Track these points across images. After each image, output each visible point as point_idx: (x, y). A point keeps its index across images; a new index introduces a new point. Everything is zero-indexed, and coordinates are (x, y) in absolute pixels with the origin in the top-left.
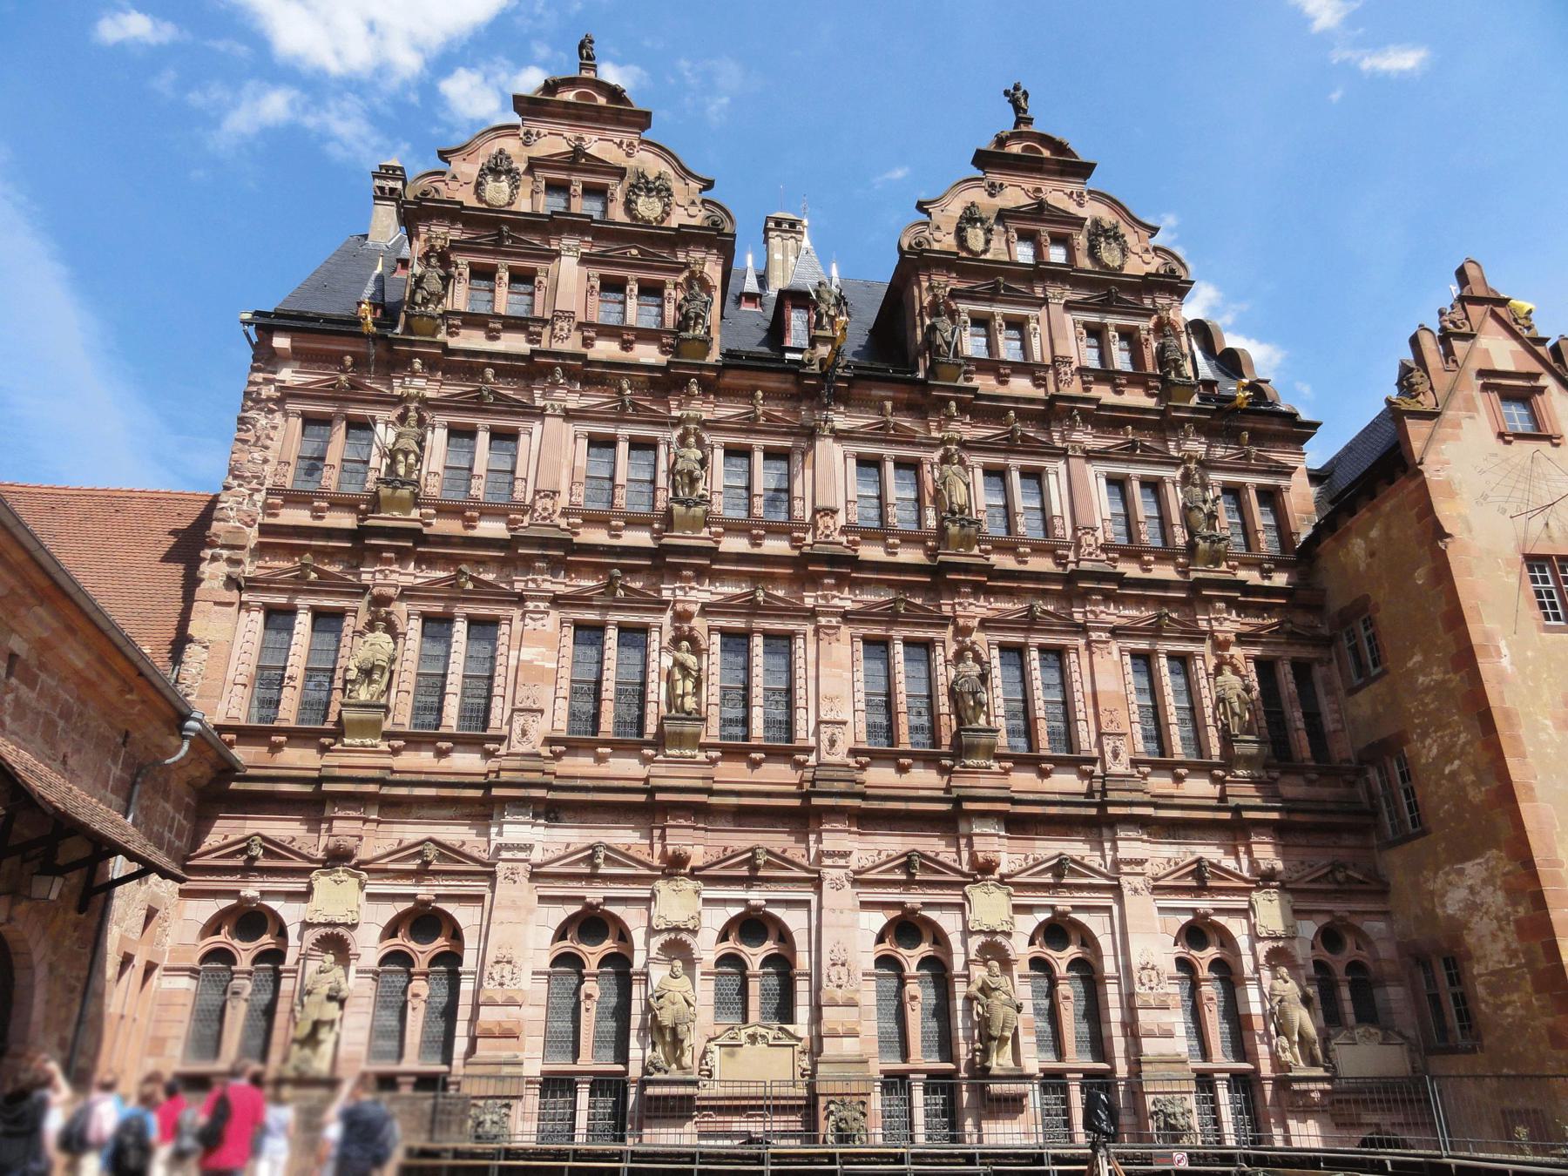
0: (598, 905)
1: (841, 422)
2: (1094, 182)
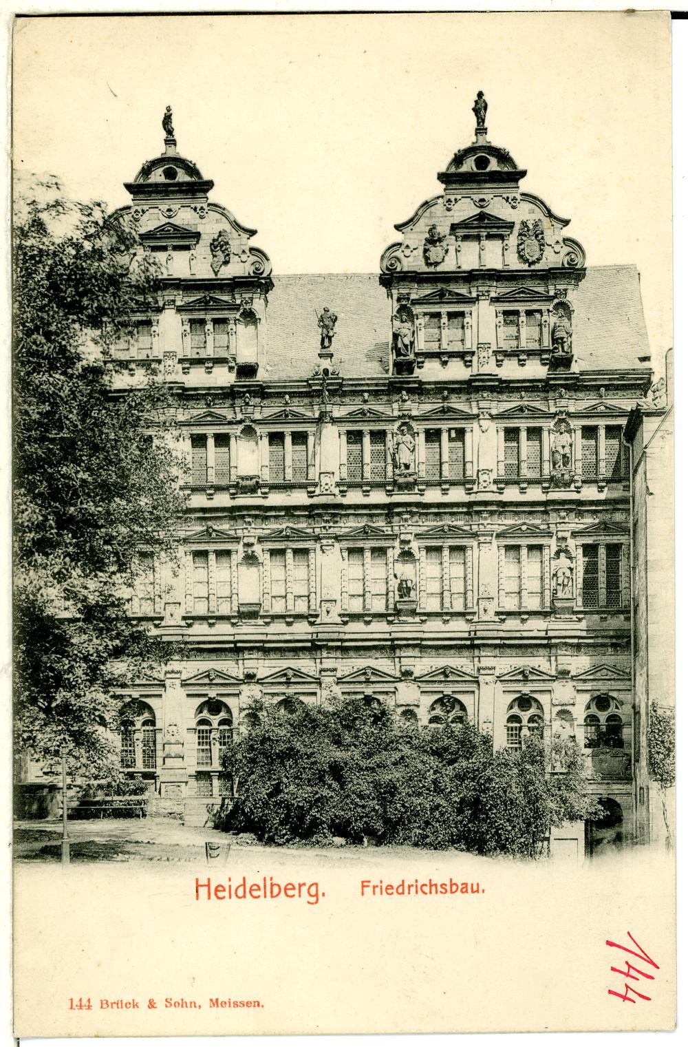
0: (214, 698)
1: (338, 412)
2: (525, 185)
